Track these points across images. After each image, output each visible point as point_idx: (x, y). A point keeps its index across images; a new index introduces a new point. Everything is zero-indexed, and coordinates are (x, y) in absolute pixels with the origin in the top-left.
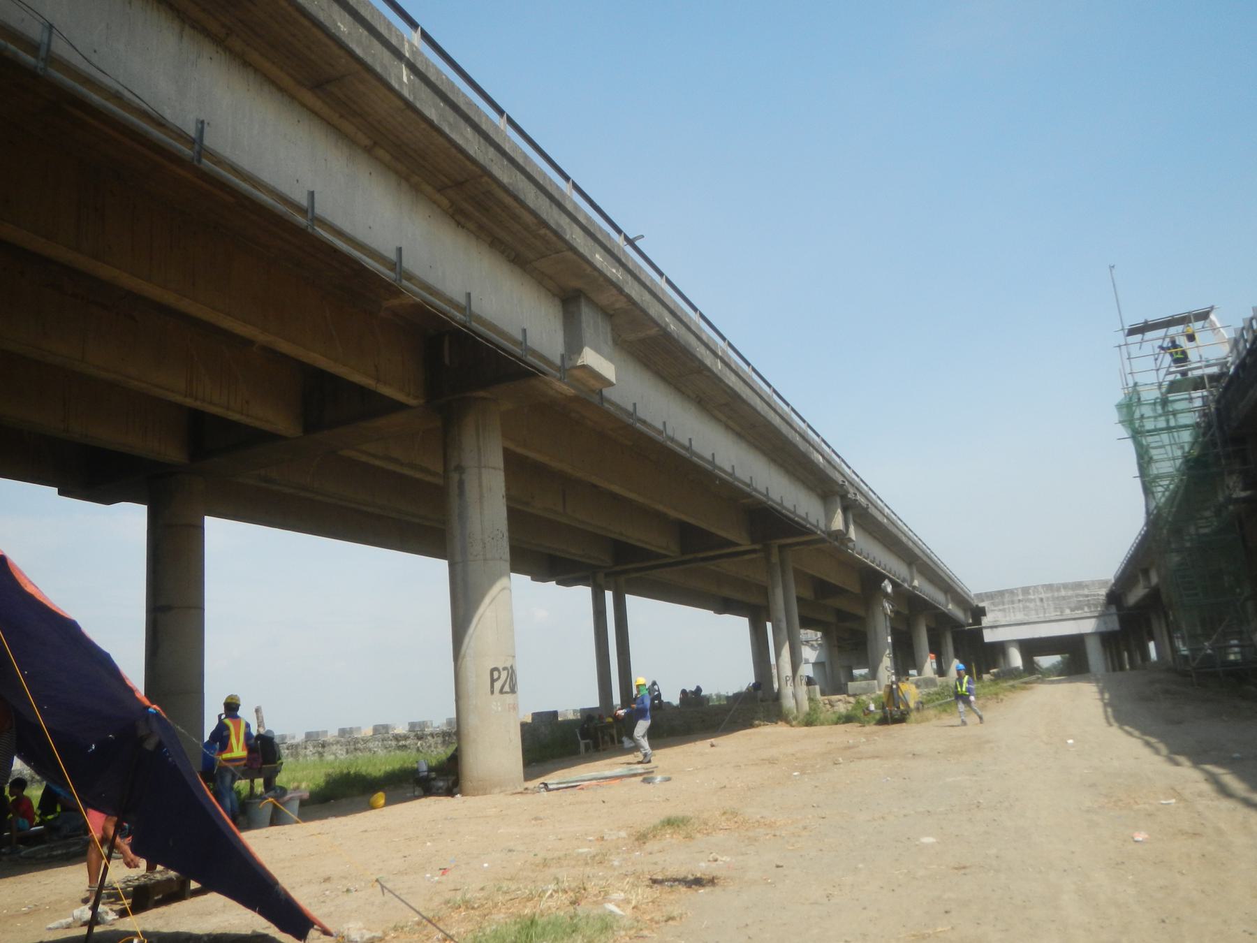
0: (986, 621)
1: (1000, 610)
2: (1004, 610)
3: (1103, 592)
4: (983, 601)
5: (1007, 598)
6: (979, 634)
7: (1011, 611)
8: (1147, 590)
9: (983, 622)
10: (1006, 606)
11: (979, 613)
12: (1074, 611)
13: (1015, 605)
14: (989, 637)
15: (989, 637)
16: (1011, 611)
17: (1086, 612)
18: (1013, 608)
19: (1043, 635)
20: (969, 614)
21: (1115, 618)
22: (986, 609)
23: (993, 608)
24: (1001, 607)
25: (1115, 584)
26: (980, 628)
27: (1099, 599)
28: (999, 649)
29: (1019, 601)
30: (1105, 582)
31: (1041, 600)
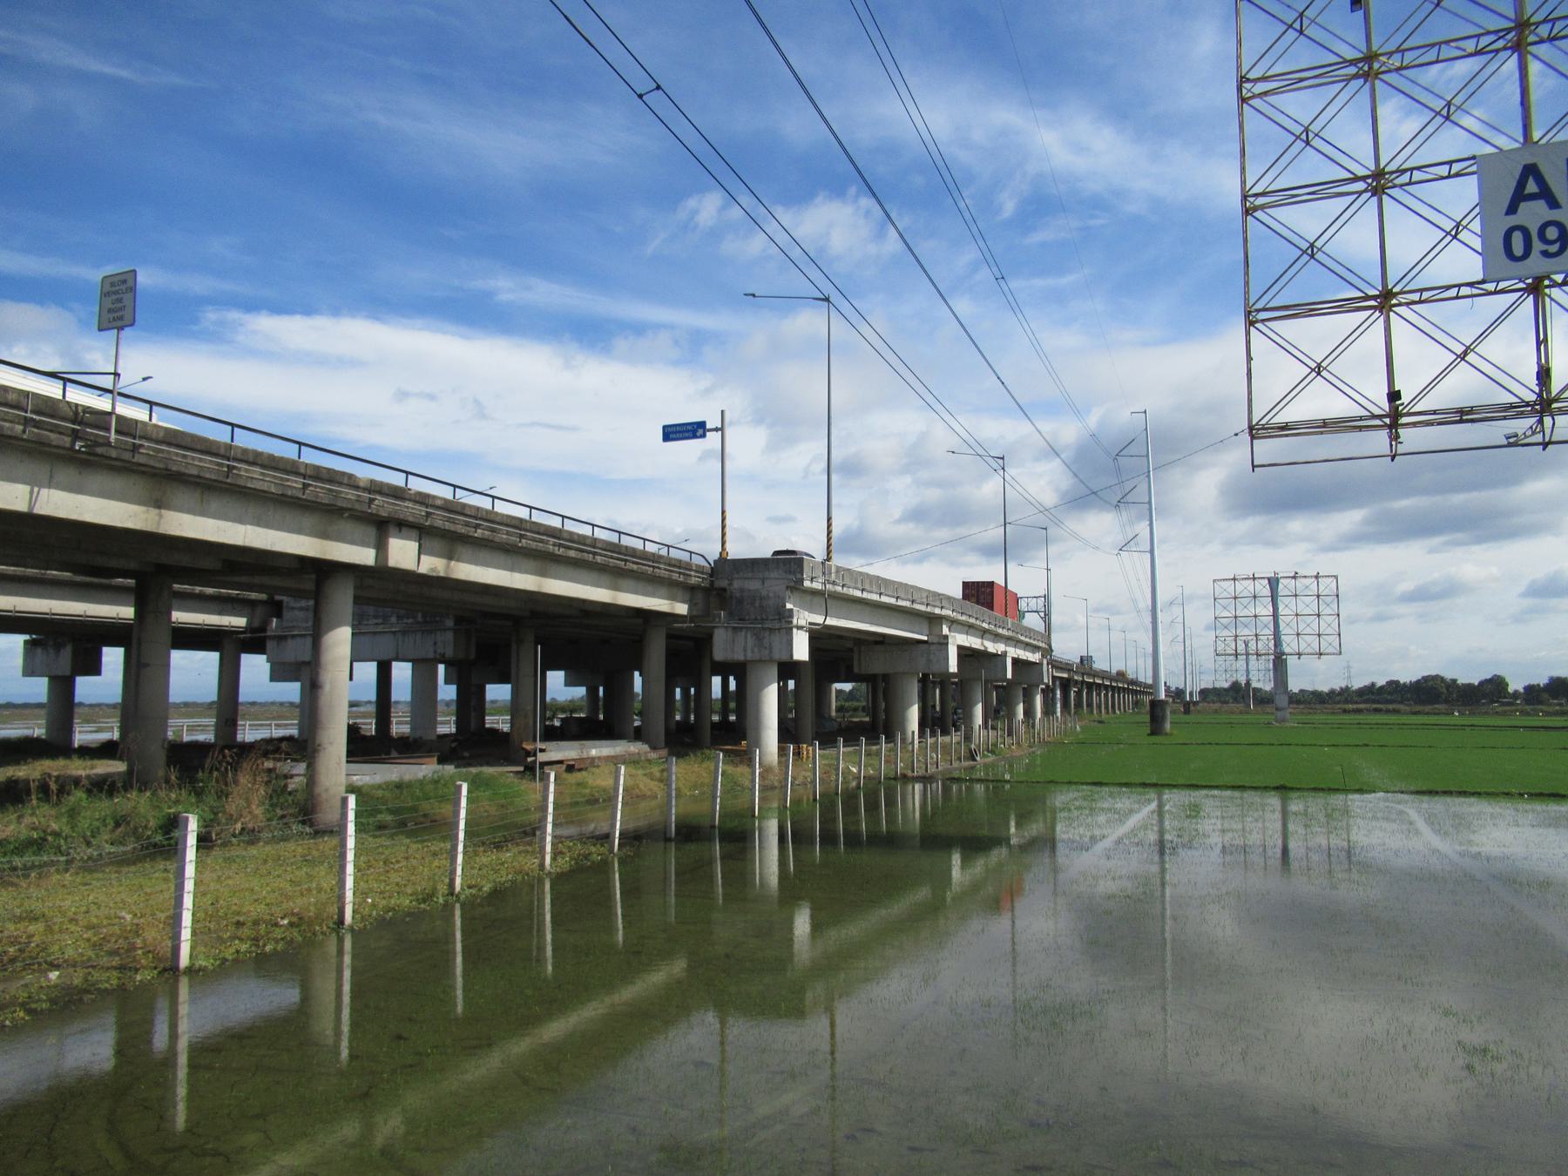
17: (418, 623)
21: (450, 636)
22: (284, 605)
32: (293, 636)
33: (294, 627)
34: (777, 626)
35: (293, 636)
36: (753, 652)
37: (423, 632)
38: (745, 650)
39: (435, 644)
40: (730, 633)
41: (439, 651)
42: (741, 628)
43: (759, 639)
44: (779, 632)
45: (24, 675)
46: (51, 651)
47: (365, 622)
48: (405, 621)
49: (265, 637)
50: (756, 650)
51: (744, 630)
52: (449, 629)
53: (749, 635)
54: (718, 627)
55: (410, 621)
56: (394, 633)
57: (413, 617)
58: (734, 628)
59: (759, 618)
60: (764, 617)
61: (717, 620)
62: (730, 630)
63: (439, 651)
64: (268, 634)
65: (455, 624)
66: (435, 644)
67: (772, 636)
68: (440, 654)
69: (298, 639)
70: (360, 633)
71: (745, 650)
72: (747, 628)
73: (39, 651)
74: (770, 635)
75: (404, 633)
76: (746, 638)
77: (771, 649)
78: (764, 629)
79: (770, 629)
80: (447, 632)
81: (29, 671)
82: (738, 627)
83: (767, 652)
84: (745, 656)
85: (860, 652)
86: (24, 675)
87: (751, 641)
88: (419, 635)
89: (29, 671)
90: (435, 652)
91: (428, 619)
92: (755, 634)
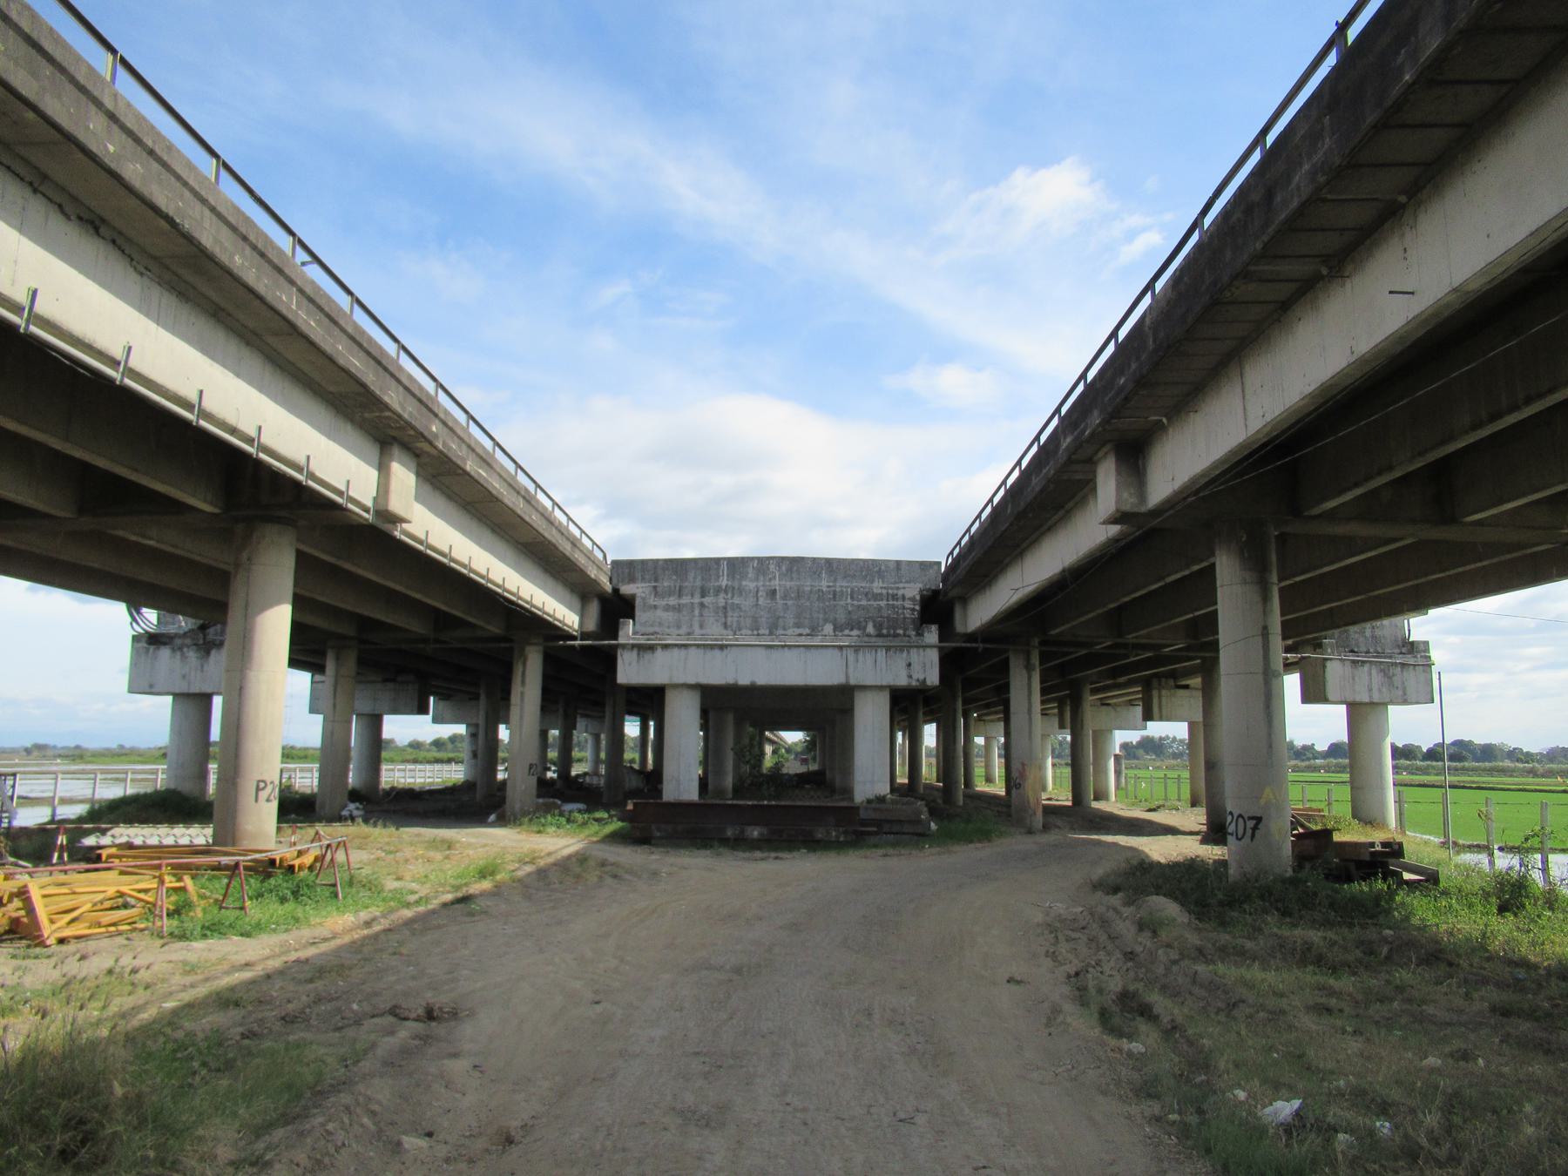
0: (628, 631)
1: (667, 608)
2: (678, 609)
3: (913, 591)
4: (632, 580)
5: (694, 580)
6: (607, 659)
7: (697, 612)
8: (1114, 530)
9: (621, 633)
10: (686, 600)
11: (615, 608)
12: (842, 631)
13: (707, 600)
14: (629, 671)
15: (629, 671)
16: (697, 612)
17: (869, 635)
18: (702, 605)
19: (762, 679)
20: (594, 608)
21: (934, 656)
22: (638, 602)
23: (652, 601)
24: (673, 601)
25: (945, 577)
26: (610, 646)
27: (904, 608)
28: (649, 701)
29: (718, 590)
30: (925, 566)
31: (772, 593)
32: (666, 647)
33: (656, 633)
34: (1412, 661)
35: (666, 647)
36: (1380, 690)
37: (888, 649)
39: (909, 665)
40: (1348, 667)
41: (915, 676)
42: (1363, 662)
43: (1389, 677)
44: (1415, 670)
45: (132, 690)
46: (192, 655)
47: (782, 632)
48: (847, 632)
49: (617, 646)
50: (1384, 690)
51: (1366, 667)
52: (931, 646)
53: (1374, 672)
54: (1331, 659)
55: (855, 632)
56: (841, 648)
57: (859, 629)
58: (1354, 662)
59: (1371, 650)
60: (1380, 650)
61: (1329, 650)
62: (1348, 663)
63: (915, 676)
64: (621, 640)
65: (940, 641)
66: (909, 665)
67: (1405, 673)
68: (918, 680)
69: (676, 650)
70: (785, 646)
72: (1371, 662)
73: (165, 652)
74: (1402, 671)
75: (857, 649)
76: (1370, 674)
78: (1393, 664)
79: (1403, 665)
80: (928, 650)
81: (141, 683)
82: (1358, 661)
83: (1400, 693)
84: (1371, 697)
85: (1160, 697)
86: (132, 690)
87: (1377, 678)
88: (881, 654)
89: (141, 683)
90: (910, 677)
91: (885, 631)
92: (1381, 671)
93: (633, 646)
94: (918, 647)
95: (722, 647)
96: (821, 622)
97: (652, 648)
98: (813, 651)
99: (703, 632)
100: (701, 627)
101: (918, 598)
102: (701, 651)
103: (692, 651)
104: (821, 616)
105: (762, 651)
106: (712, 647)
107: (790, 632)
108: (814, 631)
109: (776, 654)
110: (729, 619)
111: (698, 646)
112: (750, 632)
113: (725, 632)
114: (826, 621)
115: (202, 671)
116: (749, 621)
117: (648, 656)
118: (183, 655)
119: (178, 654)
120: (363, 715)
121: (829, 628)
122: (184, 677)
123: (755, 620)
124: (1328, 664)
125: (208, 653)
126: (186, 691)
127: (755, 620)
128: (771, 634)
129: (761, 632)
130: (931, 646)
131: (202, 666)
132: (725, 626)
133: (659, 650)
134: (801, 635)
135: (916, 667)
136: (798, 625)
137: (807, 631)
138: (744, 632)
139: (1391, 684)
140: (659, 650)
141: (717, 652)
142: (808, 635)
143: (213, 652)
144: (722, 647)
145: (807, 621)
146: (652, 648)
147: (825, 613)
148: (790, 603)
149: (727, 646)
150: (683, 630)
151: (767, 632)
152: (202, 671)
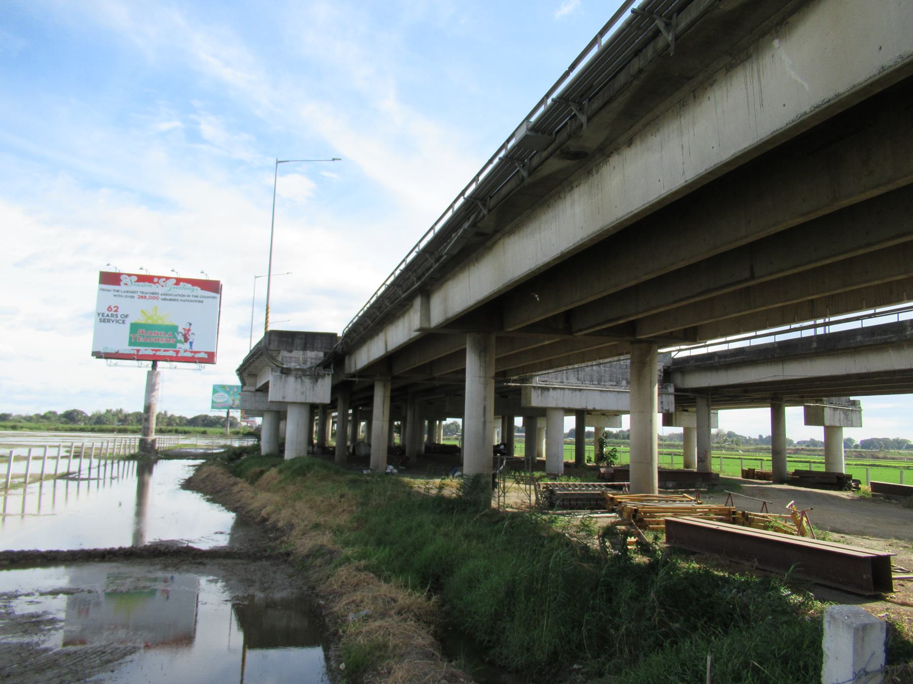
9: (533, 380)
21: (672, 398)
32: (554, 389)
38: (840, 421)
40: (832, 411)
41: (665, 408)
42: (838, 408)
43: (846, 415)
46: (307, 381)
47: (603, 383)
50: (845, 421)
51: (838, 411)
52: (671, 394)
58: (834, 408)
63: (665, 408)
68: (666, 410)
69: (559, 391)
71: (840, 421)
77: (852, 421)
79: (852, 410)
83: (850, 422)
84: (840, 424)
87: (842, 416)
93: (539, 387)
94: (666, 394)
95: (580, 390)
96: (621, 379)
97: (547, 389)
98: (621, 394)
99: (568, 381)
100: (567, 379)
101: (662, 370)
102: (570, 392)
103: (567, 392)
104: (621, 376)
105: (598, 393)
106: (575, 390)
107: (607, 383)
108: (618, 384)
109: (604, 394)
110: (580, 376)
111: (569, 389)
112: (589, 383)
113: (578, 382)
114: (623, 379)
115: (314, 390)
116: (589, 377)
117: (546, 393)
118: (302, 380)
119: (299, 380)
120: (272, 411)
121: (624, 383)
122: (303, 393)
123: (592, 376)
124: (825, 409)
125: (317, 380)
126: (304, 401)
127: (592, 376)
128: (599, 384)
129: (594, 383)
130: (671, 394)
131: (313, 388)
132: (578, 379)
133: (551, 390)
134: (612, 385)
135: (665, 403)
136: (611, 381)
137: (615, 383)
138: (586, 382)
139: (847, 419)
140: (551, 390)
141: (578, 392)
142: (615, 386)
143: (320, 380)
144: (580, 390)
145: (614, 379)
146: (547, 389)
147: (622, 375)
148: (607, 369)
149: (582, 389)
150: (559, 380)
151: (597, 383)
152: (314, 390)
